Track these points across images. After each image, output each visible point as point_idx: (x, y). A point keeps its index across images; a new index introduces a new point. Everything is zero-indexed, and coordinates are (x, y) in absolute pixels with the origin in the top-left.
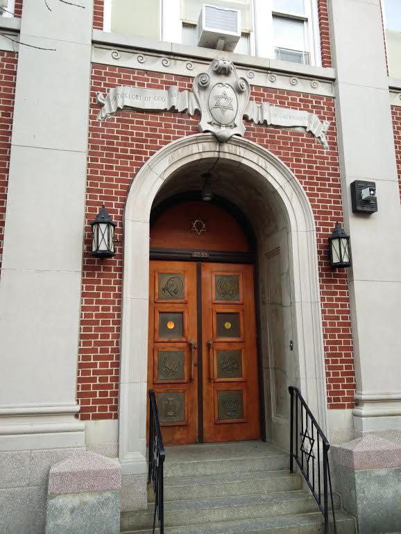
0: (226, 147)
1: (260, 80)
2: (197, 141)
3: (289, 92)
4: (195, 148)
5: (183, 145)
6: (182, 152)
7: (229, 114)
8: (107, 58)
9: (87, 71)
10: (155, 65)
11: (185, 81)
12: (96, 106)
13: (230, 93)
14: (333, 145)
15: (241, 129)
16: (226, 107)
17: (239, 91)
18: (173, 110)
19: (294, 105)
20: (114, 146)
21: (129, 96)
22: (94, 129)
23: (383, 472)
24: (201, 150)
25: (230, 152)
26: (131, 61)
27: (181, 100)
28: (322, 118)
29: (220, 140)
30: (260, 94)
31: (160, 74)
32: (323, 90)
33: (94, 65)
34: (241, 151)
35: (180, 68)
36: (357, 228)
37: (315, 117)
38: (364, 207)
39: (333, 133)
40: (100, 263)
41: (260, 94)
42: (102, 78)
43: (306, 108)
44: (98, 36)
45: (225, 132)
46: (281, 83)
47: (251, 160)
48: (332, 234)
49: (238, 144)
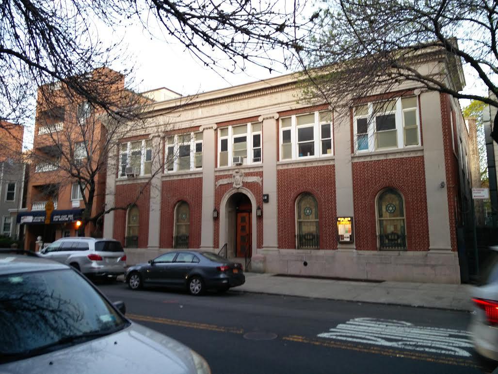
0: (239, 190)
1: (247, 171)
4: (233, 191)
6: (231, 192)
7: (238, 183)
8: (218, 174)
10: (226, 173)
11: (230, 176)
12: (216, 185)
13: (238, 177)
14: (262, 184)
15: (241, 184)
16: (238, 182)
17: (241, 176)
19: (254, 175)
20: (219, 192)
22: (216, 190)
24: (234, 191)
26: (222, 174)
28: (260, 177)
30: (247, 175)
32: (261, 170)
34: (242, 190)
35: (231, 173)
36: (265, 207)
37: (259, 177)
38: (267, 201)
39: (262, 181)
40: (216, 219)
41: (247, 175)
42: (217, 178)
43: (257, 176)
44: (216, 169)
45: (238, 186)
46: (252, 171)
47: (244, 192)
48: (260, 208)
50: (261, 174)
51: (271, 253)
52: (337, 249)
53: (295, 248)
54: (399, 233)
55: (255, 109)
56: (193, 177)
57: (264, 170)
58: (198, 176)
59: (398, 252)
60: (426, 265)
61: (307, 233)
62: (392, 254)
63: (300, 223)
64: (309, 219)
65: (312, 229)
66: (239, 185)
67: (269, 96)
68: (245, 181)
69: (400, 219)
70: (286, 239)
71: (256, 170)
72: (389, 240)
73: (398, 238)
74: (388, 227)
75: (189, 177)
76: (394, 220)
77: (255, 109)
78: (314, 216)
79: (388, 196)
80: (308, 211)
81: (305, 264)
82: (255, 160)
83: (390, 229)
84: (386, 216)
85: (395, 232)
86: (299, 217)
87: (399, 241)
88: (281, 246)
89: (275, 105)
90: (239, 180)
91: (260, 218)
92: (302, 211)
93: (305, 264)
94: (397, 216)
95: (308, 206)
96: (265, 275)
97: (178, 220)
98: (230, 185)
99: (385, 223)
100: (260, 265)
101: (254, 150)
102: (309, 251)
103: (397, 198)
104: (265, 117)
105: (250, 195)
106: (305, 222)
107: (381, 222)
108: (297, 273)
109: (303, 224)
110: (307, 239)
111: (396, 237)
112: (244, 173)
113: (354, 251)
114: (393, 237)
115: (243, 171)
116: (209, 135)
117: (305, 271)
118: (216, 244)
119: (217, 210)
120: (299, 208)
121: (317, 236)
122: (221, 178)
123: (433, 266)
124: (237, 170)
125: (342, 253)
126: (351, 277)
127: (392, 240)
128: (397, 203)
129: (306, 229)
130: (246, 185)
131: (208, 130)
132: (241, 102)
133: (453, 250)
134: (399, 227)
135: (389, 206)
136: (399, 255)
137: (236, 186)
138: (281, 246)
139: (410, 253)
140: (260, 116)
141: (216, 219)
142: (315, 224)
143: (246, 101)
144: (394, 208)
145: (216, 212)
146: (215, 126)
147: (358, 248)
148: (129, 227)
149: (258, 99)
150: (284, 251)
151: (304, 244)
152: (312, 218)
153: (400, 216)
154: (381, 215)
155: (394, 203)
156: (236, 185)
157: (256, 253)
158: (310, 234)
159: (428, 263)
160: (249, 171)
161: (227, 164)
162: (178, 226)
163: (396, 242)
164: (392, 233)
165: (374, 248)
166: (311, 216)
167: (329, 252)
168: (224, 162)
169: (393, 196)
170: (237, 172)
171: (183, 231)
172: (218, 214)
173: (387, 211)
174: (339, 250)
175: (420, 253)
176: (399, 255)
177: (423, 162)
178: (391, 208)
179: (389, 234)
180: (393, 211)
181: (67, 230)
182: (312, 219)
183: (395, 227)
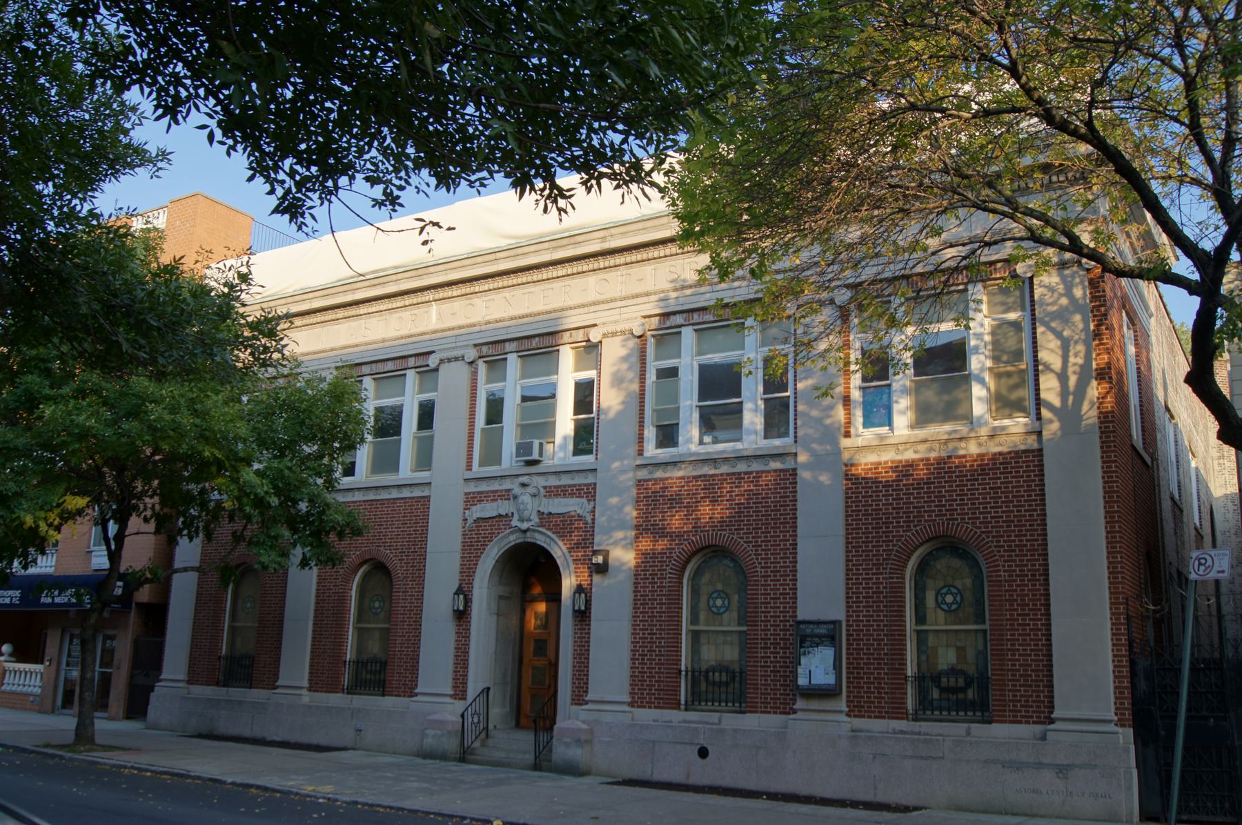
0: (528, 534)
1: (553, 481)
2: (512, 533)
3: (570, 486)
4: (512, 538)
5: (504, 537)
7: (526, 514)
8: (472, 488)
9: (462, 498)
10: (495, 486)
11: (506, 495)
13: (526, 498)
18: (500, 516)
19: (572, 495)
21: (478, 511)
23: (568, 740)
24: (514, 539)
25: (529, 538)
26: (484, 487)
27: (503, 507)
29: (525, 531)
30: (552, 492)
31: (496, 491)
32: (590, 479)
33: (466, 494)
34: (537, 536)
35: (507, 485)
37: (584, 500)
41: (552, 492)
42: (472, 499)
44: (469, 475)
45: (525, 526)
46: (565, 481)
47: (541, 540)
49: (534, 531)
50: (589, 492)
51: (607, 718)
52: (795, 712)
53: (677, 706)
54: (971, 670)
55: (583, 306)
56: (406, 493)
57: (600, 479)
58: (417, 493)
59: (966, 725)
60: (1039, 766)
61: (713, 663)
62: (946, 731)
63: (695, 636)
64: (721, 625)
65: (730, 654)
66: (529, 520)
67: (622, 270)
68: (546, 512)
69: (976, 631)
70: (653, 684)
71: (580, 480)
72: (942, 690)
73: (969, 683)
74: (941, 651)
75: (395, 494)
76: (957, 631)
77: (583, 306)
78: (735, 615)
79: (944, 563)
80: (719, 602)
81: (703, 753)
82: (577, 451)
83: (946, 658)
84: (937, 621)
85: (959, 667)
86: (694, 619)
87: (970, 694)
88: (638, 701)
89: (637, 296)
90: (529, 507)
91: (583, 616)
92: (703, 599)
93: (703, 753)
94: (968, 623)
95: (720, 587)
96: (586, 780)
97: (360, 618)
98: (504, 518)
99: (931, 640)
100: (576, 754)
101: (576, 421)
102: (715, 717)
103: (967, 570)
104: (610, 329)
105: (559, 550)
106: (707, 631)
107: (921, 636)
108: (677, 776)
109: (703, 639)
110: (714, 684)
111: (961, 682)
112: (545, 488)
113: (844, 718)
114: (952, 682)
115: (541, 482)
116: (453, 379)
117: (702, 773)
118: (460, 691)
119: (464, 591)
120: (695, 592)
121: (741, 673)
122: (481, 501)
123: (1062, 770)
124: (524, 479)
125: (807, 723)
126: (828, 794)
127: (955, 690)
128: (968, 582)
129: (710, 655)
130: (546, 519)
131: (452, 364)
132: (546, 285)
133: (1121, 723)
134: (971, 654)
135: (944, 591)
136: (968, 733)
137: (519, 524)
138: (638, 701)
139: (1000, 730)
140: (595, 325)
141: (462, 616)
142: (735, 638)
143: (557, 285)
144: (958, 598)
145: (461, 597)
146: (472, 354)
147: (856, 710)
148: (233, 629)
149: (592, 279)
150: (646, 715)
151: (704, 697)
152: (730, 623)
153: (976, 623)
154: (920, 618)
155: (958, 583)
156: (521, 520)
157: (569, 718)
158: (721, 668)
159: (1046, 760)
160: (558, 483)
161: (499, 462)
162: (361, 633)
163: (961, 696)
164: (953, 671)
165: (897, 712)
166: (726, 616)
167: (772, 721)
168: (492, 454)
169: (956, 563)
170: (524, 485)
171: (374, 648)
172: (468, 601)
173: (938, 605)
174: (799, 715)
175: (1024, 731)
176: (968, 733)
177: (1041, 466)
178: (949, 599)
179: (940, 675)
180: (954, 607)
181: (110, 632)
182: (729, 625)
183: (961, 651)
